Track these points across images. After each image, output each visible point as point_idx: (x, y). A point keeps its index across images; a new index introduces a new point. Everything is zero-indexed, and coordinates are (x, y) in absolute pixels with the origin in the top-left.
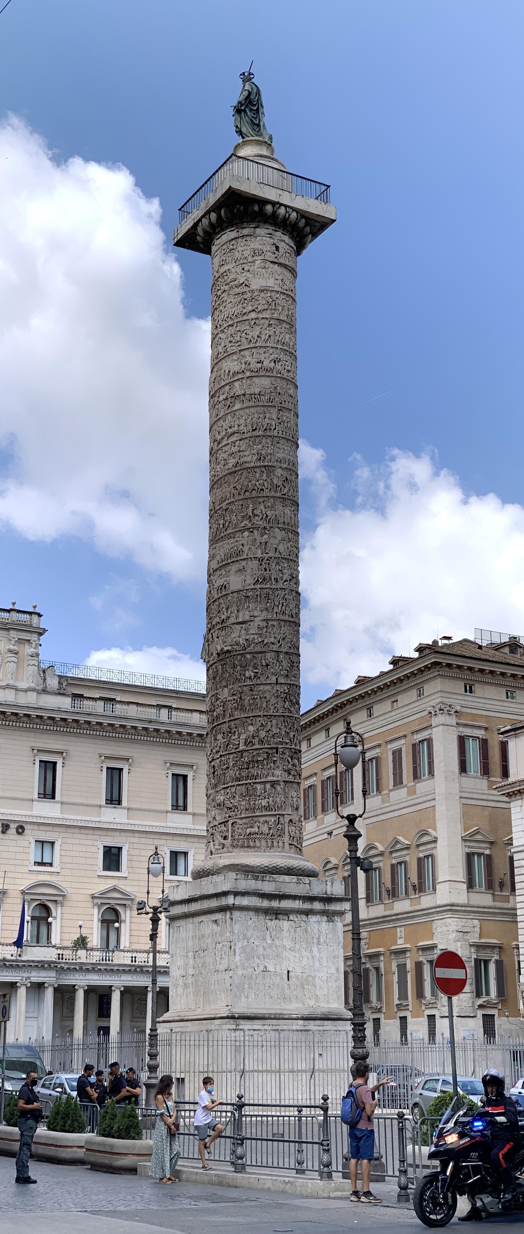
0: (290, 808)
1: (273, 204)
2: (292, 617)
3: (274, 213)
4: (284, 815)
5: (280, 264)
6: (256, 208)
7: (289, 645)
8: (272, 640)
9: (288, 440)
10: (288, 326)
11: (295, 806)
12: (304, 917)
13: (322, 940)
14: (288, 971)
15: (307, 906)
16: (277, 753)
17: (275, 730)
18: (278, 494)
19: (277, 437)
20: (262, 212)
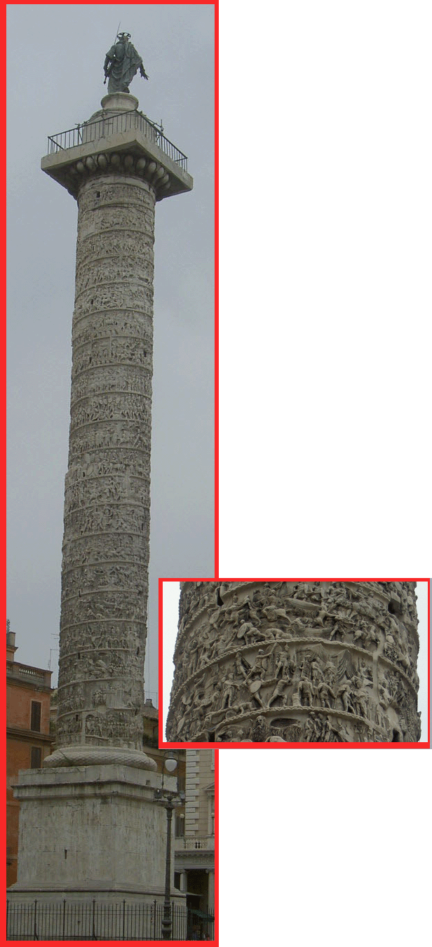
0: (91, 705)
1: (80, 160)
2: (101, 530)
3: (85, 166)
4: (81, 712)
5: (100, 208)
6: (73, 171)
7: (96, 557)
8: (78, 557)
9: (103, 367)
10: (110, 261)
11: (97, 699)
12: (80, 801)
13: (96, 821)
14: (66, 851)
15: (77, 792)
16: (79, 658)
17: (78, 638)
18: (90, 421)
19: (91, 369)
20: (79, 173)
